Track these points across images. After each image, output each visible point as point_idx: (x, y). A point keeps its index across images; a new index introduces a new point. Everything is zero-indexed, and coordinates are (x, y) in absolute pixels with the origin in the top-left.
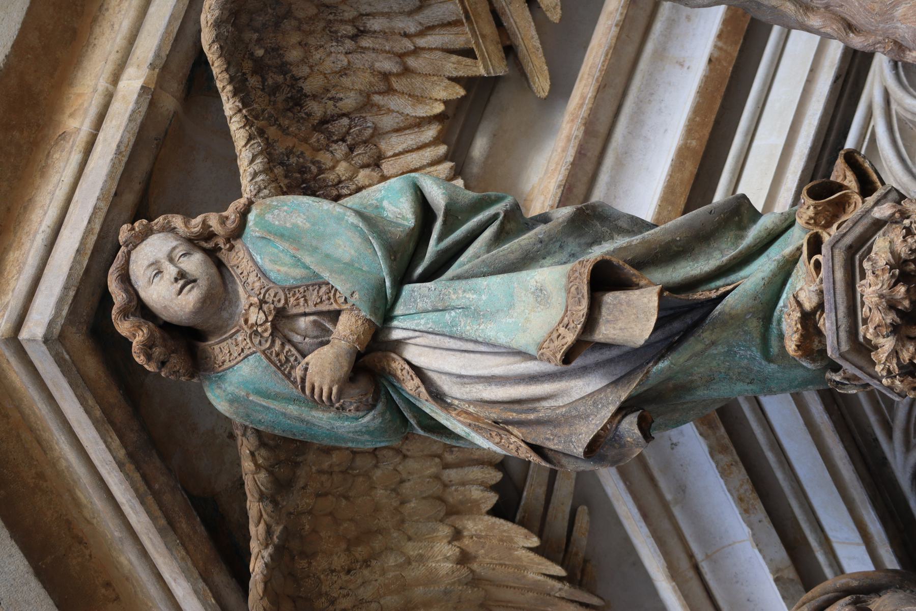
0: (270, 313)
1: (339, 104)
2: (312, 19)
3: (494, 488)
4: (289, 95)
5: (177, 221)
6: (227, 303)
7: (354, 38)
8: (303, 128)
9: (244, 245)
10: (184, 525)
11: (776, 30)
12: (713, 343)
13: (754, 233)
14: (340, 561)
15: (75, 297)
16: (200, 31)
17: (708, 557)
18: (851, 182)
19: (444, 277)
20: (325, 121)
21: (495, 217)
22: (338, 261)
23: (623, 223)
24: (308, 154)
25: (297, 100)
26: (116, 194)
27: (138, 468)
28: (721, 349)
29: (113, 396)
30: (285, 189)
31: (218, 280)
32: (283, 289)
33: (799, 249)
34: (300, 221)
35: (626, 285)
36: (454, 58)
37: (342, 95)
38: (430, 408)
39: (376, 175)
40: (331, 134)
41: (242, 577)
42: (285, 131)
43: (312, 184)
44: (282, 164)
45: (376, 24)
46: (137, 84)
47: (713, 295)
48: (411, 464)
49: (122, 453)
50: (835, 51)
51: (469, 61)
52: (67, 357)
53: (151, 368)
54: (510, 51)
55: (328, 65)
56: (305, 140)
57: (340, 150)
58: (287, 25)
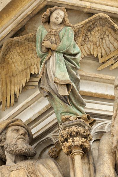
2: (103, 31)
3: (35, 73)
5: (67, 15)
7: (101, 38)
10: (19, 26)
11: (113, 104)
12: (62, 105)
13: (81, 108)
14: (19, 51)
15: (51, 2)
16: (98, 13)
17: (31, 108)
18: (91, 121)
19: (65, 61)
20: (87, 36)
21: (76, 66)
23: (78, 87)
25: (89, 31)
27: (27, 17)
28: (61, 106)
29: (37, 11)
31: (58, 24)
33: (79, 115)
35: (68, 90)
36: (101, 54)
38: (44, 61)
41: (13, 36)
42: (84, 30)
44: (79, 30)
45: (104, 41)
46: (87, 5)
47: (69, 103)
48: (36, 59)
49: (28, 14)
50: (111, 114)
51: (101, 57)
53: (43, 16)
54: (104, 63)
55: (96, 35)
57: (83, 39)
58: (101, 27)
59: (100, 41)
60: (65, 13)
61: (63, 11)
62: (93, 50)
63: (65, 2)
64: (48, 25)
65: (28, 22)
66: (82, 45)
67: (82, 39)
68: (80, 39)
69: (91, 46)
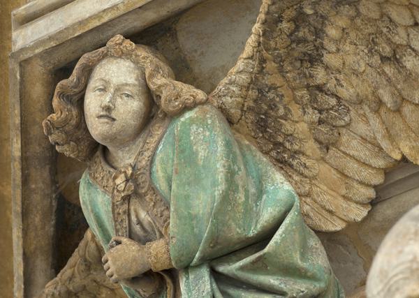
0: (128, 191)
1: (339, 88)
4: (309, 52)
6: (127, 148)
7: (384, 59)
8: (298, 81)
9: (167, 128)
10: (37, 219)
20: (320, 88)
22: (188, 207)
24: (286, 99)
25: (313, 59)
26: (140, 8)
27: (23, 170)
30: (245, 109)
31: (130, 131)
32: (151, 182)
34: (202, 154)
37: (345, 85)
39: (319, 153)
40: (315, 100)
42: (281, 70)
43: (270, 120)
44: (260, 91)
52: (18, 77)
55: (350, 59)
56: (293, 89)
59: (389, 80)
60: (136, 63)
61: (123, 55)
62: (390, 136)
63: (112, 8)
64: (103, 163)
65: (54, 182)
66: (326, 146)
67: (306, 118)
68: (299, 124)
69: (367, 122)
